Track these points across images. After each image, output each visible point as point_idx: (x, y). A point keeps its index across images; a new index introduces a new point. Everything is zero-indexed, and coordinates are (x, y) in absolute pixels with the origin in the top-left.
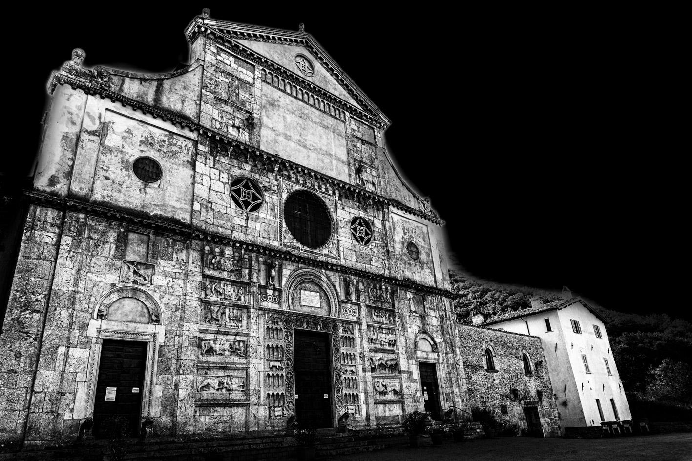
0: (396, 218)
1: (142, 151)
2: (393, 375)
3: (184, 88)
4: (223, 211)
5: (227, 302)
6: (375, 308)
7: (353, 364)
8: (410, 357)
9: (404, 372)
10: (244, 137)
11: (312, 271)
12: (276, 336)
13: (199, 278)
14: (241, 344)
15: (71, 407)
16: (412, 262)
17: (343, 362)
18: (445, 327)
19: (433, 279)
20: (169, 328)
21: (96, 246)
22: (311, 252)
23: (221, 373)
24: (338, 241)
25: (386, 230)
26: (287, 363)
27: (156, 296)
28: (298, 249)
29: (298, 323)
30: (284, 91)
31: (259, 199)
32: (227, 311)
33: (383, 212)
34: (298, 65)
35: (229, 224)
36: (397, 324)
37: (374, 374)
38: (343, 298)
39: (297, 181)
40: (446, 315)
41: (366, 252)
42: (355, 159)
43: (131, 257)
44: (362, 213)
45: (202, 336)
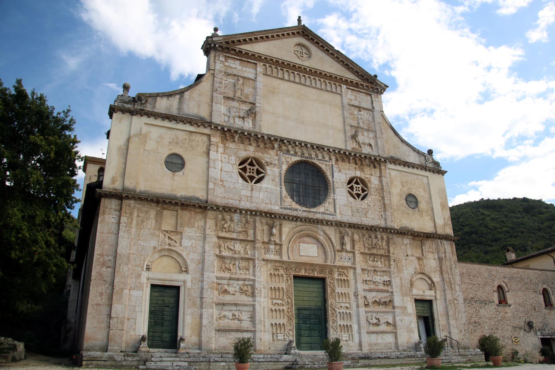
0: (393, 173)
1: (170, 149)
2: (387, 310)
3: (200, 95)
4: (232, 186)
5: (236, 256)
6: (370, 255)
7: (348, 301)
8: (404, 295)
9: (398, 307)
10: (248, 125)
11: (309, 227)
12: (277, 280)
13: (215, 240)
14: (249, 287)
15: (134, 327)
16: (409, 212)
17: (337, 300)
18: (444, 267)
19: (433, 225)
20: (194, 276)
21: (143, 222)
22: (309, 212)
23: (234, 308)
24: (334, 200)
25: (382, 185)
26: (287, 301)
27: (184, 254)
28: (296, 210)
29: (297, 270)
30: (283, 79)
31: (263, 173)
32: (237, 263)
33: (380, 170)
34: (296, 52)
35: (237, 196)
37: (367, 309)
38: (338, 247)
39: (296, 154)
40: (445, 257)
41: (363, 207)
42: (351, 126)
43: (165, 227)
44: (359, 172)
45: (219, 281)
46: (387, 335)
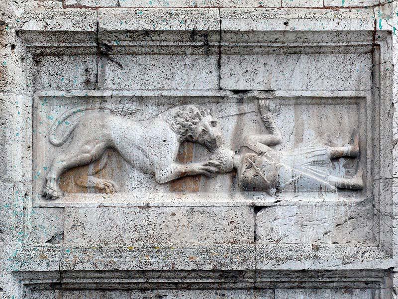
23: (196, 77)
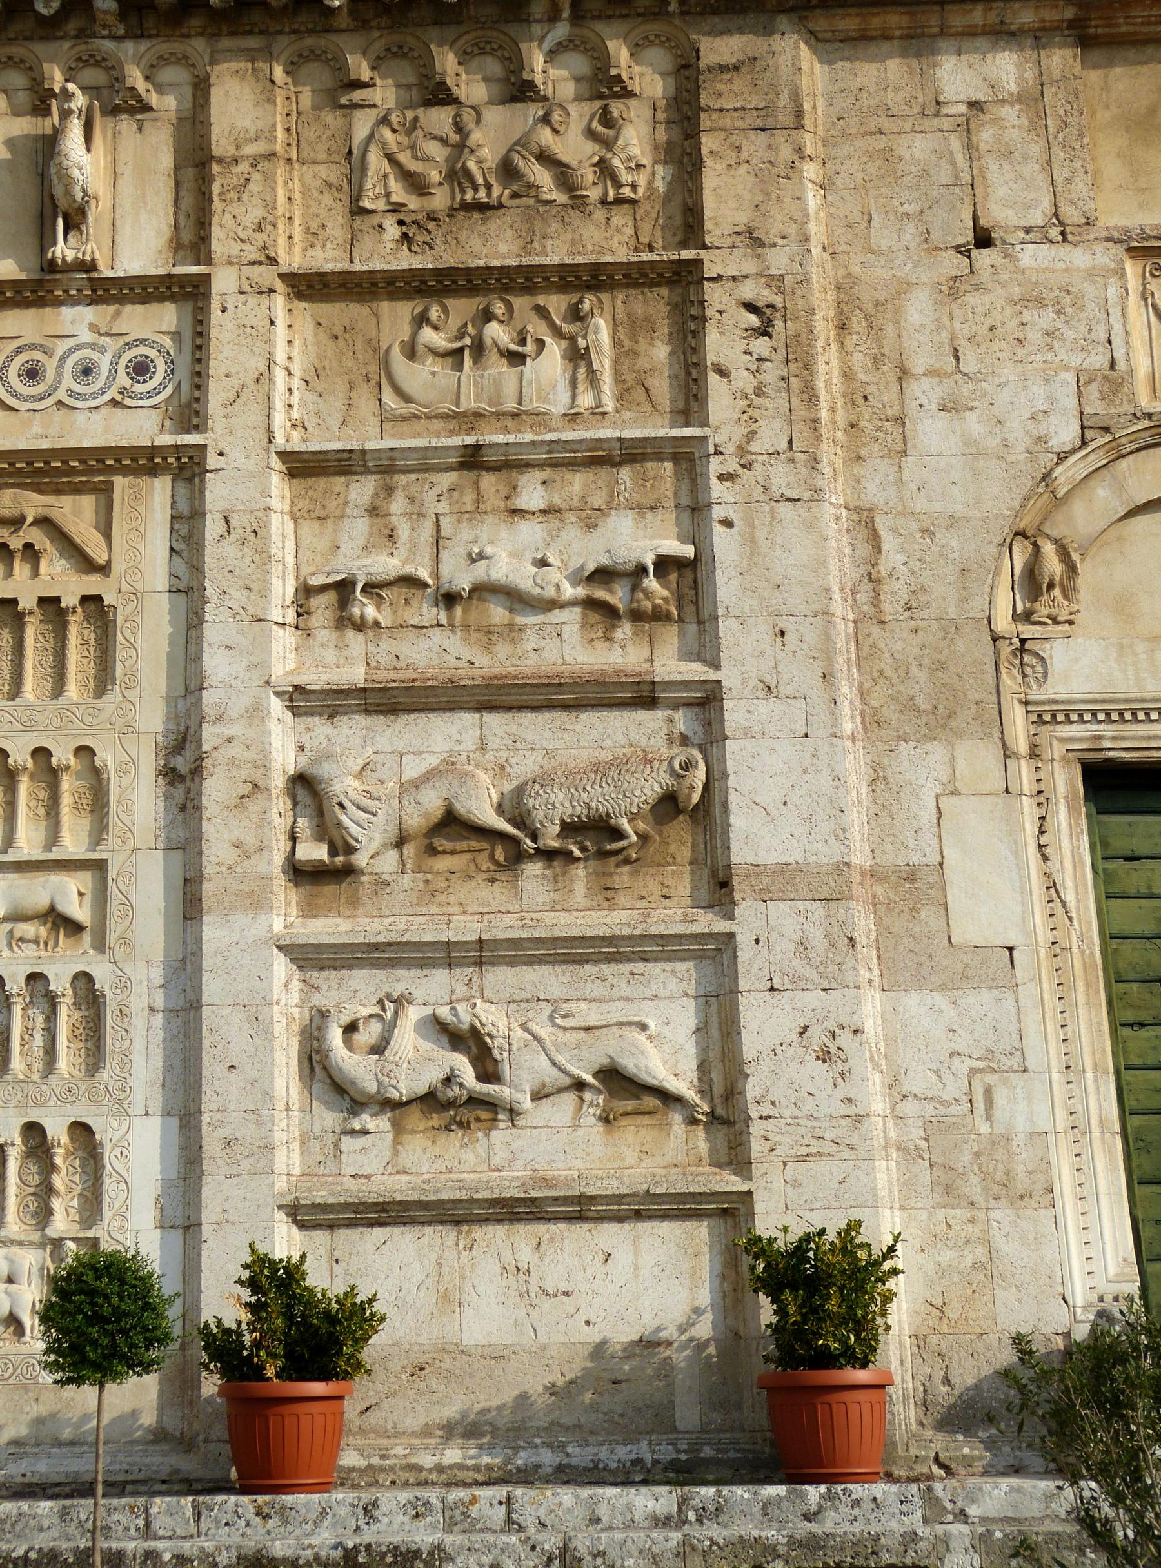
2: (618, 920)
7: (73, 844)
9: (782, 881)
36: (721, 400)
46: (609, 1234)
